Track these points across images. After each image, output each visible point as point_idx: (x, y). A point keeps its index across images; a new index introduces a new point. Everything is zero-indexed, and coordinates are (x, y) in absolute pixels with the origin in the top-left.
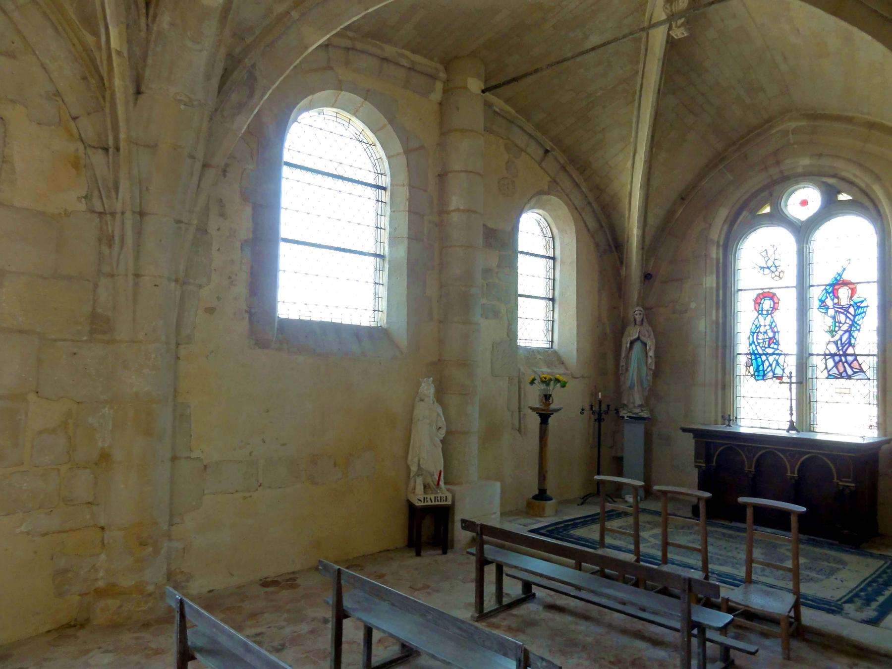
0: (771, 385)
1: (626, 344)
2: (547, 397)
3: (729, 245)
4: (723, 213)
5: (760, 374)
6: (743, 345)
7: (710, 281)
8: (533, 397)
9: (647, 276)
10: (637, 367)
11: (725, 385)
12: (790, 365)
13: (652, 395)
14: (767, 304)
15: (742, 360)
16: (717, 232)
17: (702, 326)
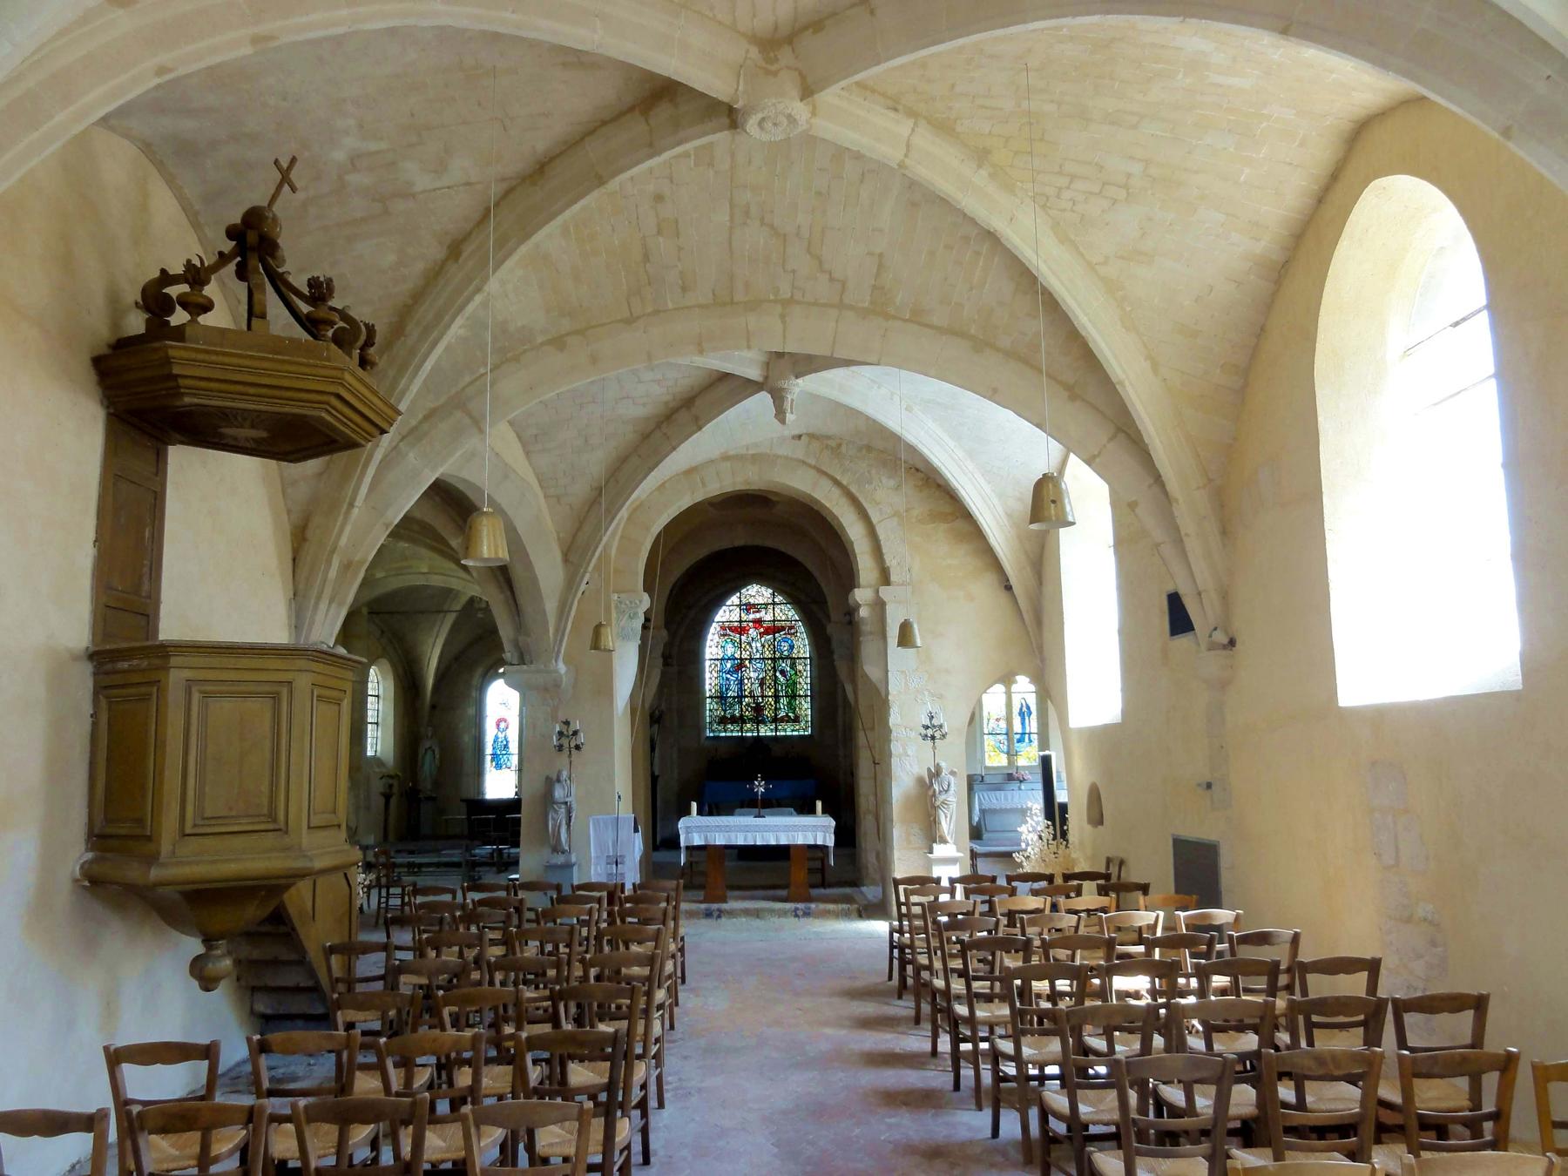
0: (505, 771)
1: (421, 751)
2: (391, 786)
3: (482, 690)
4: (480, 671)
5: (498, 767)
6: (489, 750)
7: (471, 711)
8: (378, 786)
9: (433, 707)
10: (428, 766)
11: (479, 774)
12: (515, 760)
13: (437, 784)
14: (502, 725)
15: (488, 758)
16: (476, 681)
17: (467, 739)
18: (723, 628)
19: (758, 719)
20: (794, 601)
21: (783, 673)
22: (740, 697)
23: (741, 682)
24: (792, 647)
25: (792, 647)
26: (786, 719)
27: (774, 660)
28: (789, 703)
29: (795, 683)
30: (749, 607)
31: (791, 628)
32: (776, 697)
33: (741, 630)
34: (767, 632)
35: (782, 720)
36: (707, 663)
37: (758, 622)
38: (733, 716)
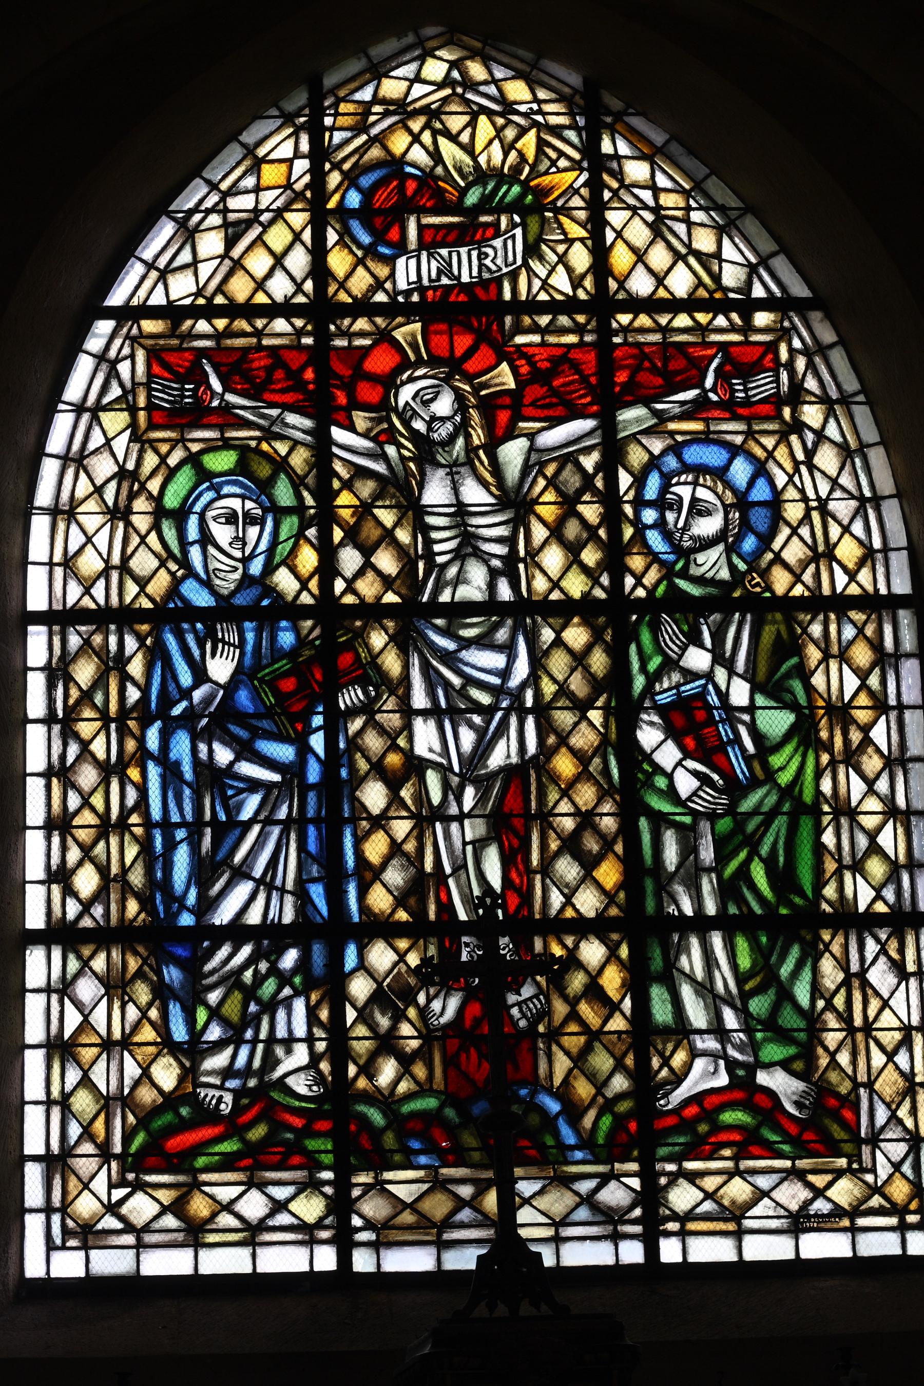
18: (173, 361)
19: (490, 1113)
20: (740, 176)
21: (693, 722)
22: (329, 934)
23: (326, 810)
24: (754, 518)
25: (754, 518)
26: (746, 1126)
27: (614, 618)
28: (763, 976)
29: (801, 809)
30: (393, 203)
31: (741, 364)
32: (644, 929)
33: (322, 371)
34: (548, 390)
35: (698, 1134)
36: (38, 646)
37: (469, 317)
38: (262, 1094)
